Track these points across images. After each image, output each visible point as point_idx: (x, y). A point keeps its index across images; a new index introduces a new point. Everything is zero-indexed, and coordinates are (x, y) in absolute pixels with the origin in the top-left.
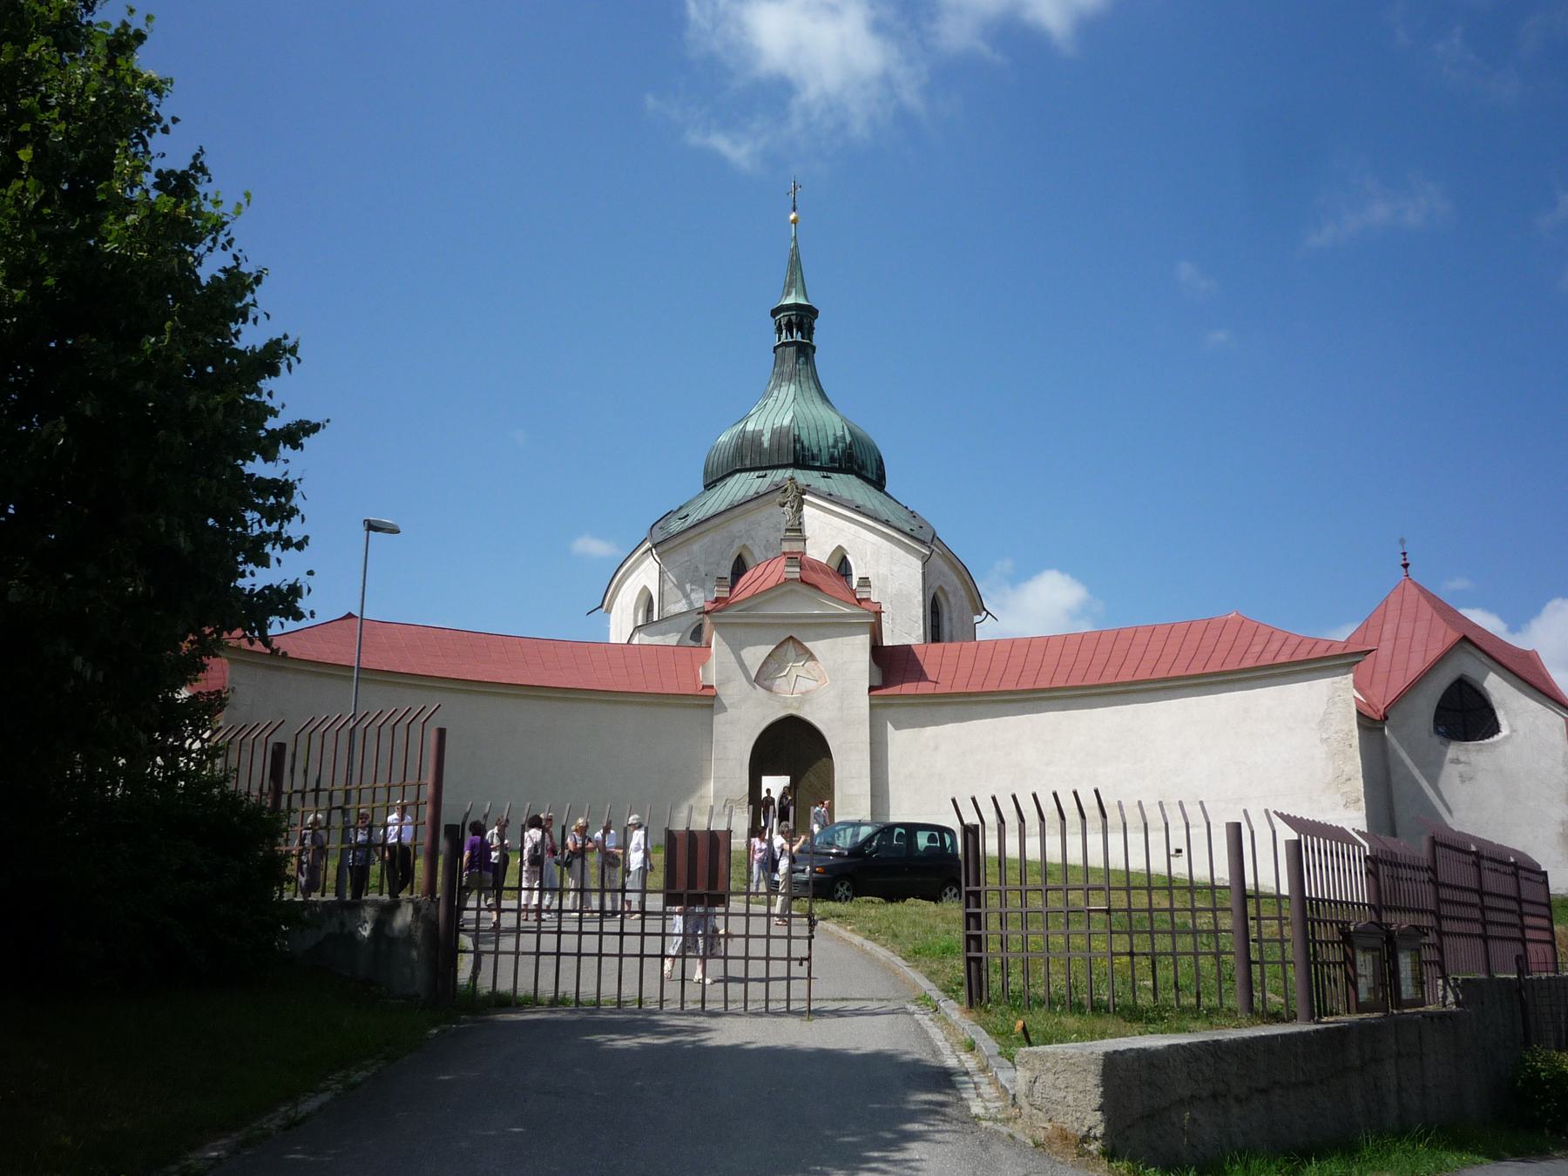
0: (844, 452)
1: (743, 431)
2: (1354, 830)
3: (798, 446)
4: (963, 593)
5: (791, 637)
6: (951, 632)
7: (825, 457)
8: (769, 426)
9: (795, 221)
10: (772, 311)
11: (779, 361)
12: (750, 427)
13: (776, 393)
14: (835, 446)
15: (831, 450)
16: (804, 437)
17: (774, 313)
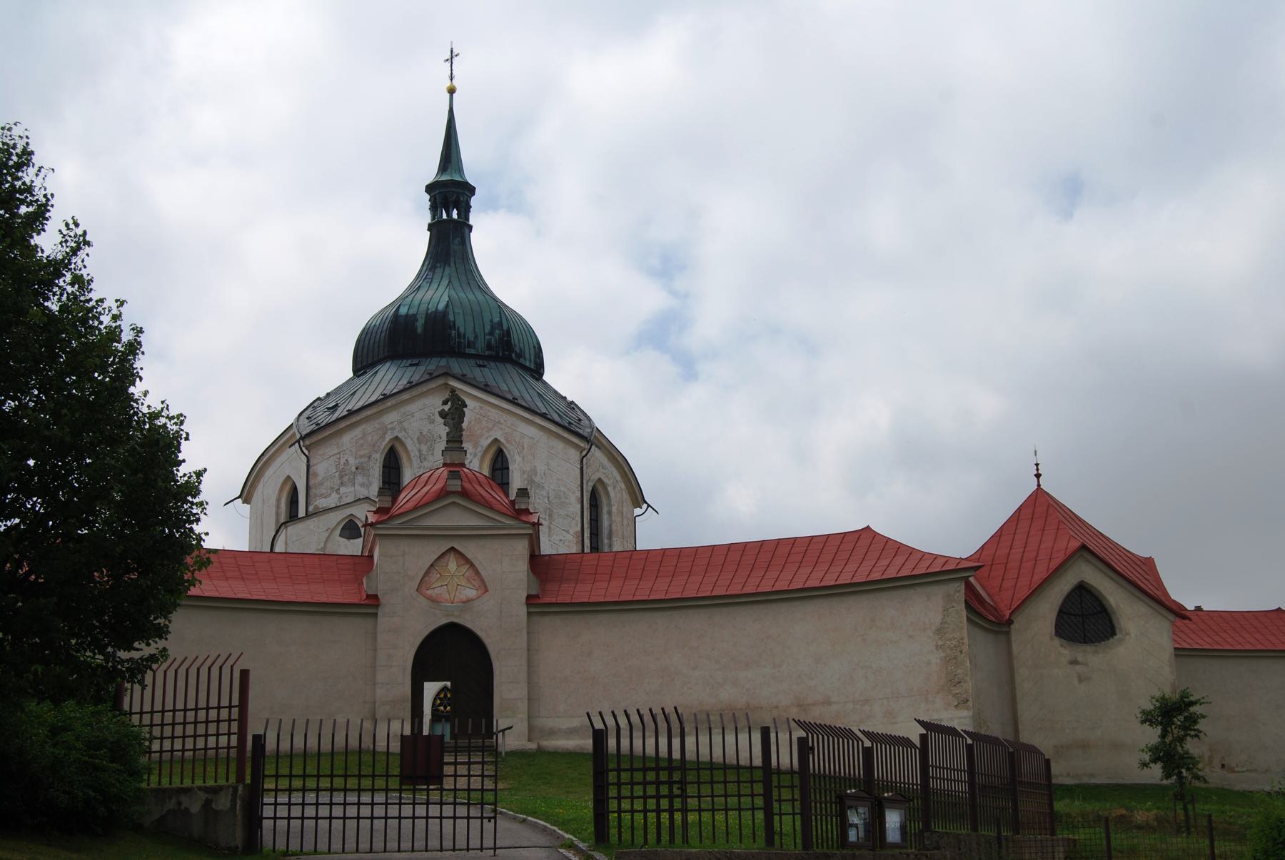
2: (962, 730)
4: (623, 486)
5: (453, 549)
6: (610, 526)
7: (481, 345)
10: (427, 186)
14: (491, 333)
15: (487, 337)
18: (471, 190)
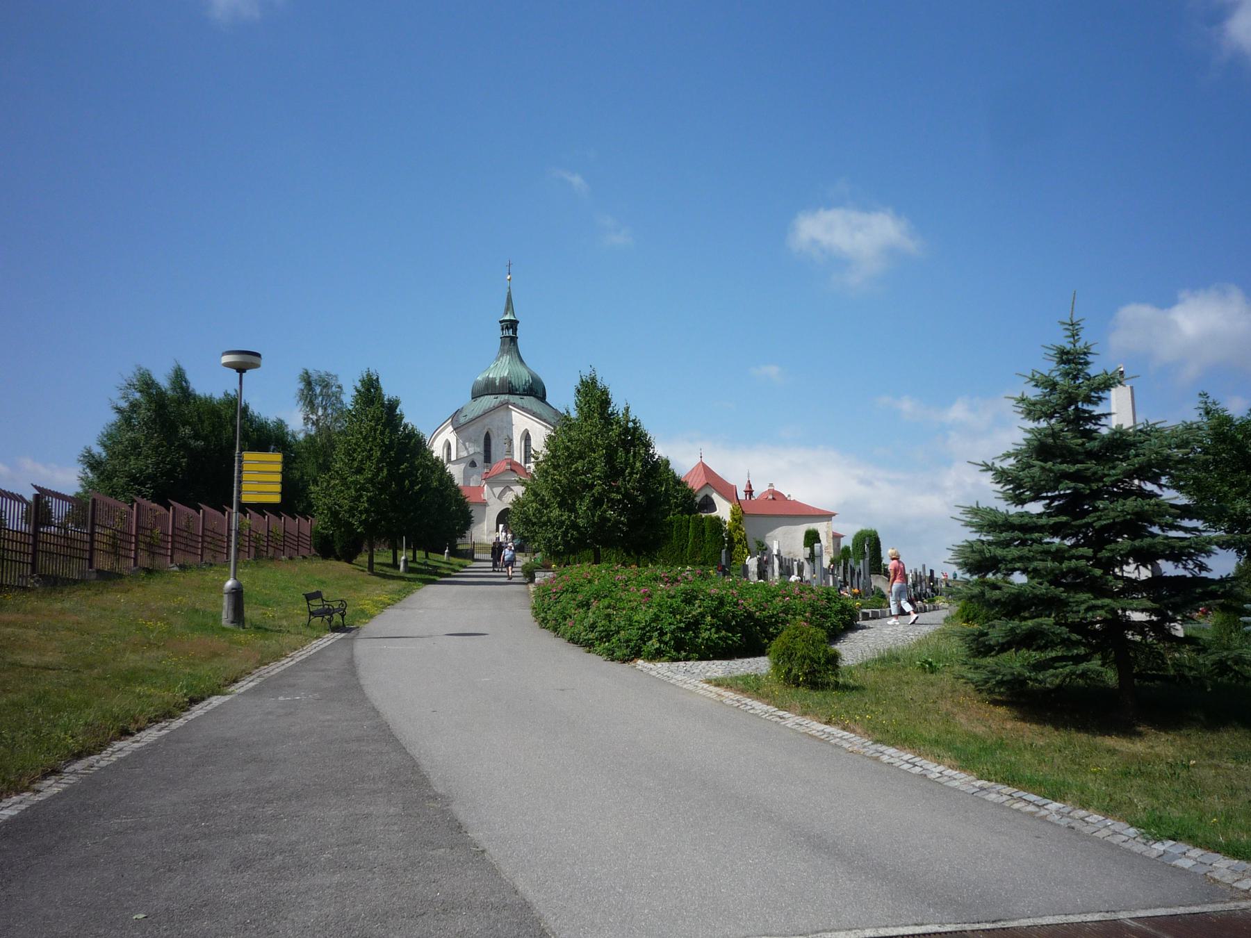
0: (529, 386)
1: (488, 377)
3: (510, 385)
7: (521, 389)
8: (498, 376)
9: (509, 280)
11: (503, 344)
12: (491, 376)
13: (501, 359)
16: (513, 382)
17: (501, 322)
18: (518, 322)
